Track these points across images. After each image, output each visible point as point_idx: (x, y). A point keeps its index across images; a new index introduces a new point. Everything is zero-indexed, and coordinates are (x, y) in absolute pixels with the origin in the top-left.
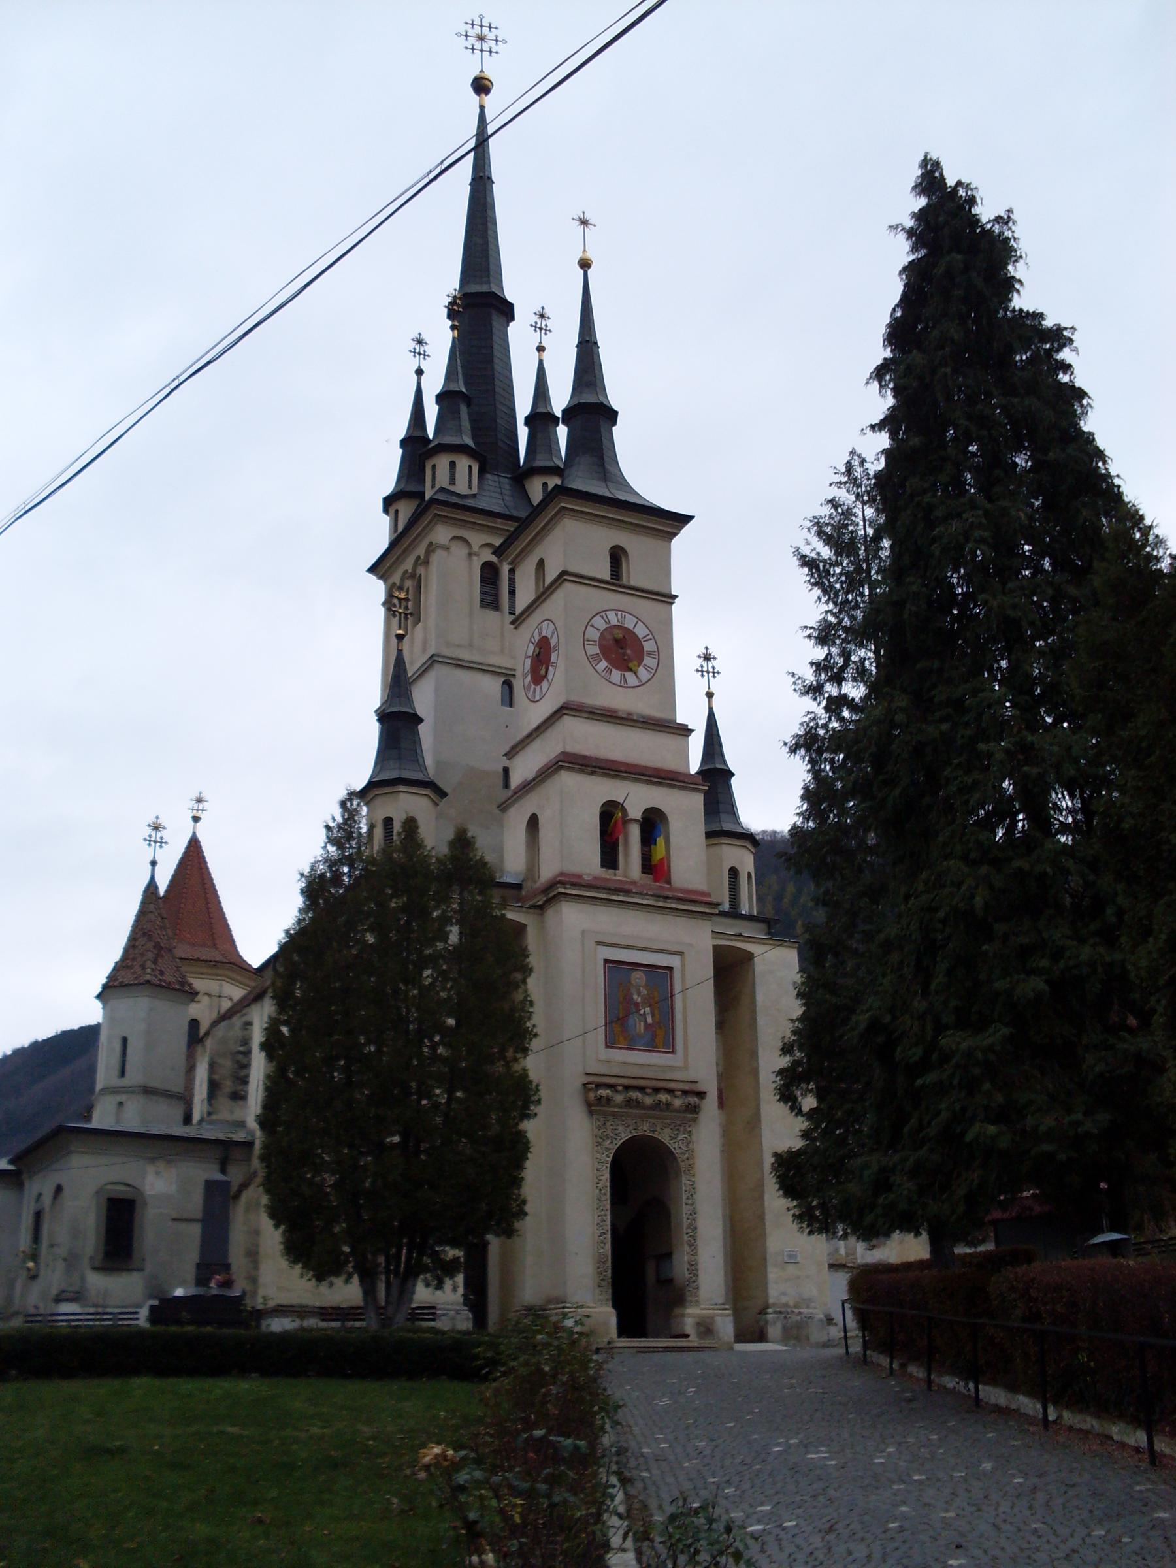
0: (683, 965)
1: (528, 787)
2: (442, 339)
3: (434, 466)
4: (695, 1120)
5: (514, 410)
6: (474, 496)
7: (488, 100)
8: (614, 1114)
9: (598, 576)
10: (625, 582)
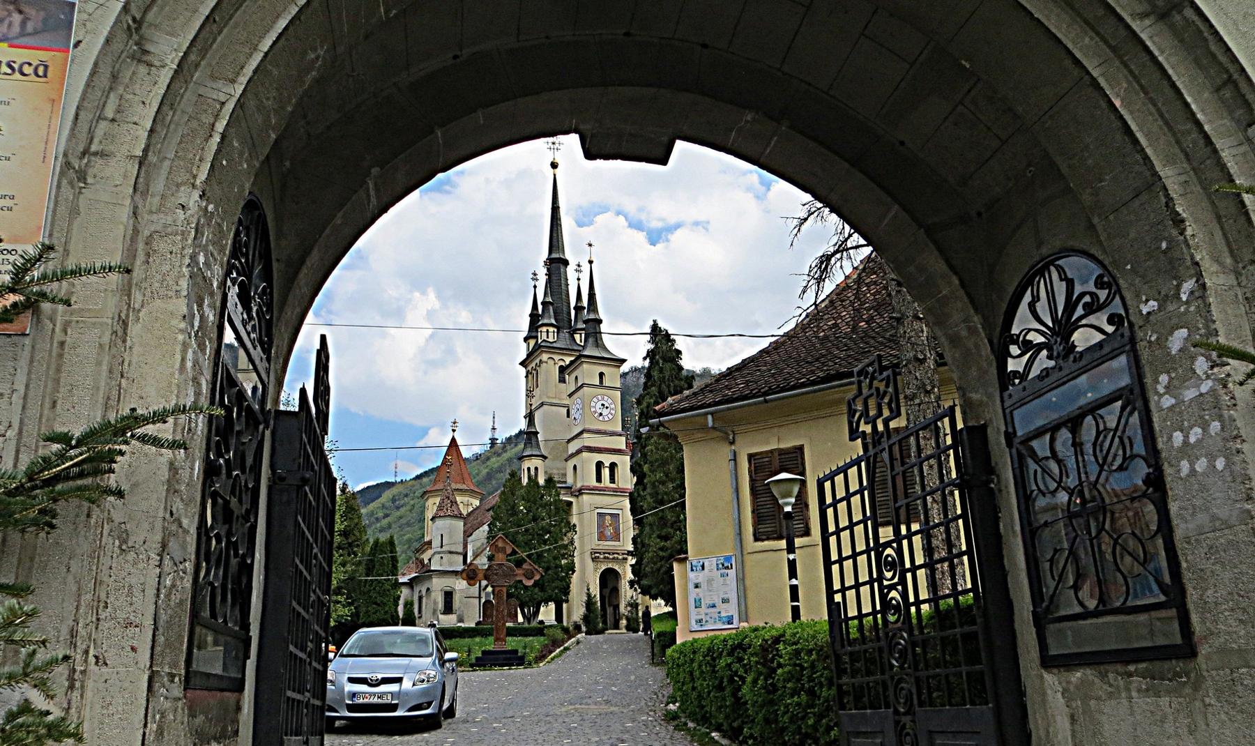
1: (573, 455)
2: (542, 279)
7: (557, 171)
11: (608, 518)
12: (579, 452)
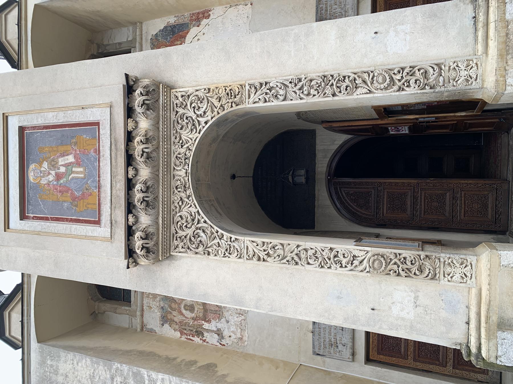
0: (18, 113)
4: (169, 88)
8: (167, 227)
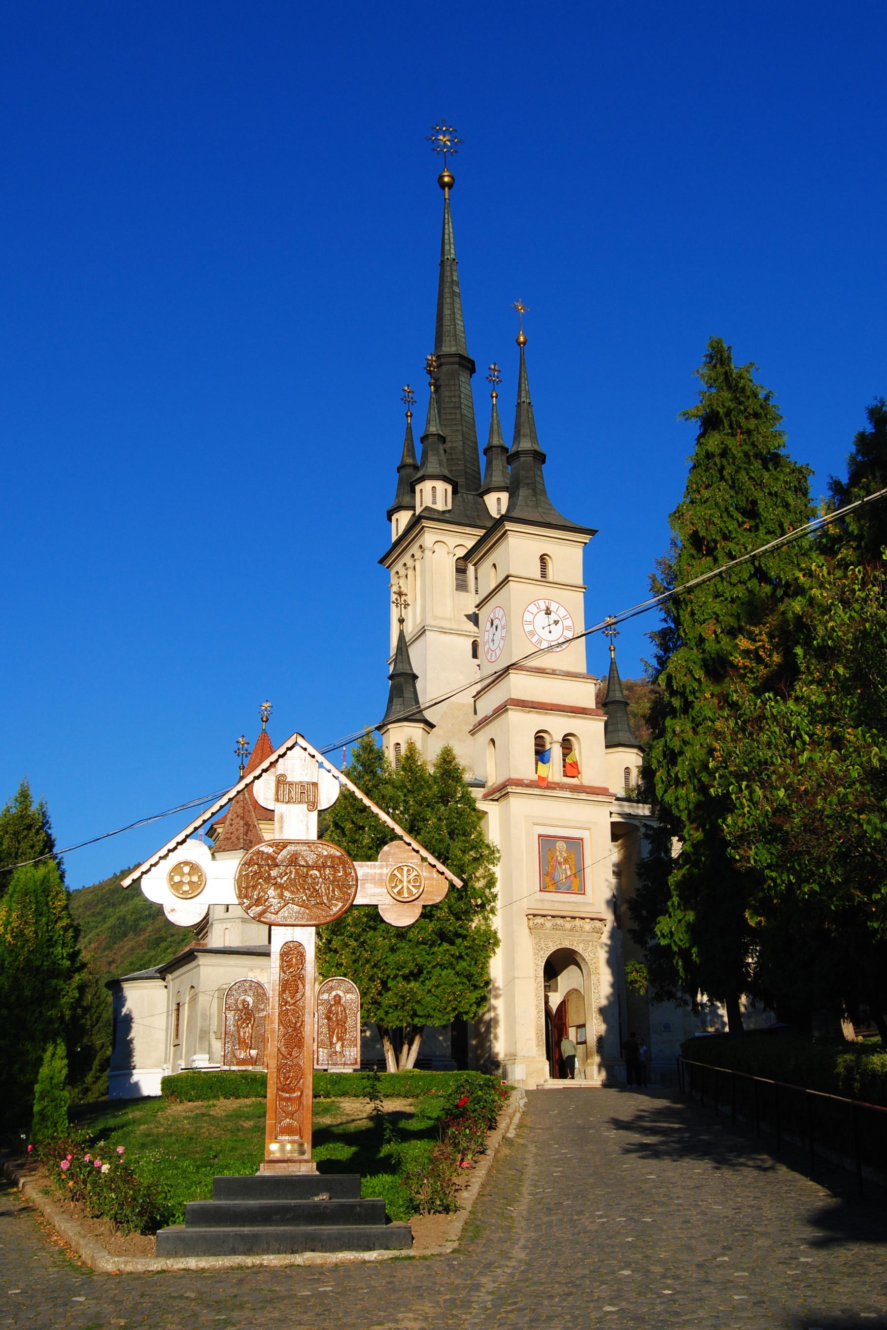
3: (421, 490)
5: (476, 443)
6: (449, 511)
9: (532, 577)
10: (551, 579)
11: (561, 845)
12: (501, 710)
